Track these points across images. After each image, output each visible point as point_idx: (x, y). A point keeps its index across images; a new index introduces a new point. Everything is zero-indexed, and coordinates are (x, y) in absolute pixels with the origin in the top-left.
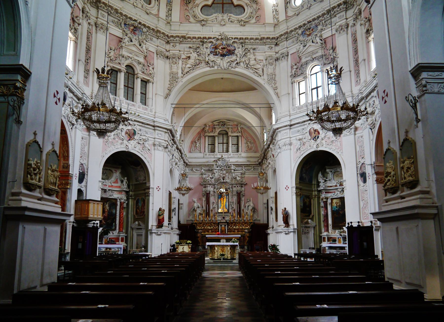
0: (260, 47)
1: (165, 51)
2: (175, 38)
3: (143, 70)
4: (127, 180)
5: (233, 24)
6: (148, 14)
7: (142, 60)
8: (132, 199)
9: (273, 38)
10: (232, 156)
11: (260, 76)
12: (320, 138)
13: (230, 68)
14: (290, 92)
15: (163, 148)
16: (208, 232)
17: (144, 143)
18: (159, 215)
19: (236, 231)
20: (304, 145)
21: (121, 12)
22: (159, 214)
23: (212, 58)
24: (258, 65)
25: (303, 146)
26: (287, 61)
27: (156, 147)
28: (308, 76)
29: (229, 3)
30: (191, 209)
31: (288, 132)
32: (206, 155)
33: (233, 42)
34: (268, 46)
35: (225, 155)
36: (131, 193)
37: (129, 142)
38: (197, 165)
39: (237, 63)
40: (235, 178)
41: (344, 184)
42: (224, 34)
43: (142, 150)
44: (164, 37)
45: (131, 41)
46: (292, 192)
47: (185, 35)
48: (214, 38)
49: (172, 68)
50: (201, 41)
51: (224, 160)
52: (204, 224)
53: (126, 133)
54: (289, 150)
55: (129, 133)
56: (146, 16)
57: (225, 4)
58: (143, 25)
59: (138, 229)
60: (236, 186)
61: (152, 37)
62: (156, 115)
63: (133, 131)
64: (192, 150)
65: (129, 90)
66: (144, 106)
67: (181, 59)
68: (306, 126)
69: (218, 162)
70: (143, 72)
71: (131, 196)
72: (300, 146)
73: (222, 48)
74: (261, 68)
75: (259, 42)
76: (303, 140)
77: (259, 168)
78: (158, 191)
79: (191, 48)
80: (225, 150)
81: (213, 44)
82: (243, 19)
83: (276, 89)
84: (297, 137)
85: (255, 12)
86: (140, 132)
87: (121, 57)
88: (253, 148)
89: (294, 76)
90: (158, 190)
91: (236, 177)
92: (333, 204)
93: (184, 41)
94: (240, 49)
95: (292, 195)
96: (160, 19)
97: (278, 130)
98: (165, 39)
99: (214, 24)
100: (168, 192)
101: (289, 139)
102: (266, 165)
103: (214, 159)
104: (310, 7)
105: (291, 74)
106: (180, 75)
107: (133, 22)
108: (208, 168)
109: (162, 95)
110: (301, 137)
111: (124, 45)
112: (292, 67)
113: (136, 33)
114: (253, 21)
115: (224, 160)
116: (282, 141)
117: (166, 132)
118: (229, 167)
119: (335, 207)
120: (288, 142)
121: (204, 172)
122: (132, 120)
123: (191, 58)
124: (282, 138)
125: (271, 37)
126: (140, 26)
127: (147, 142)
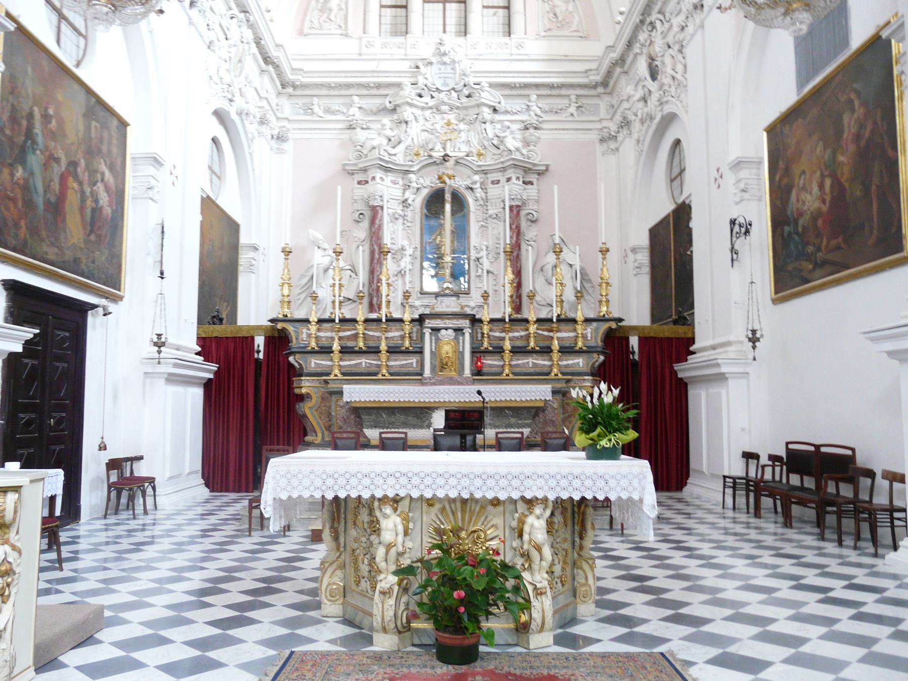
32: (369, 45)
38: (329, 86)
51: (446, 59)
60: (503, 180)
64: (307, 24)
69: (423, 69)
77: (603, 104)
80: (451, 27)
88: (576, 20)
91: (501, 140)
115: (446, 59)
118: (469, 96)
121: (358, 115)
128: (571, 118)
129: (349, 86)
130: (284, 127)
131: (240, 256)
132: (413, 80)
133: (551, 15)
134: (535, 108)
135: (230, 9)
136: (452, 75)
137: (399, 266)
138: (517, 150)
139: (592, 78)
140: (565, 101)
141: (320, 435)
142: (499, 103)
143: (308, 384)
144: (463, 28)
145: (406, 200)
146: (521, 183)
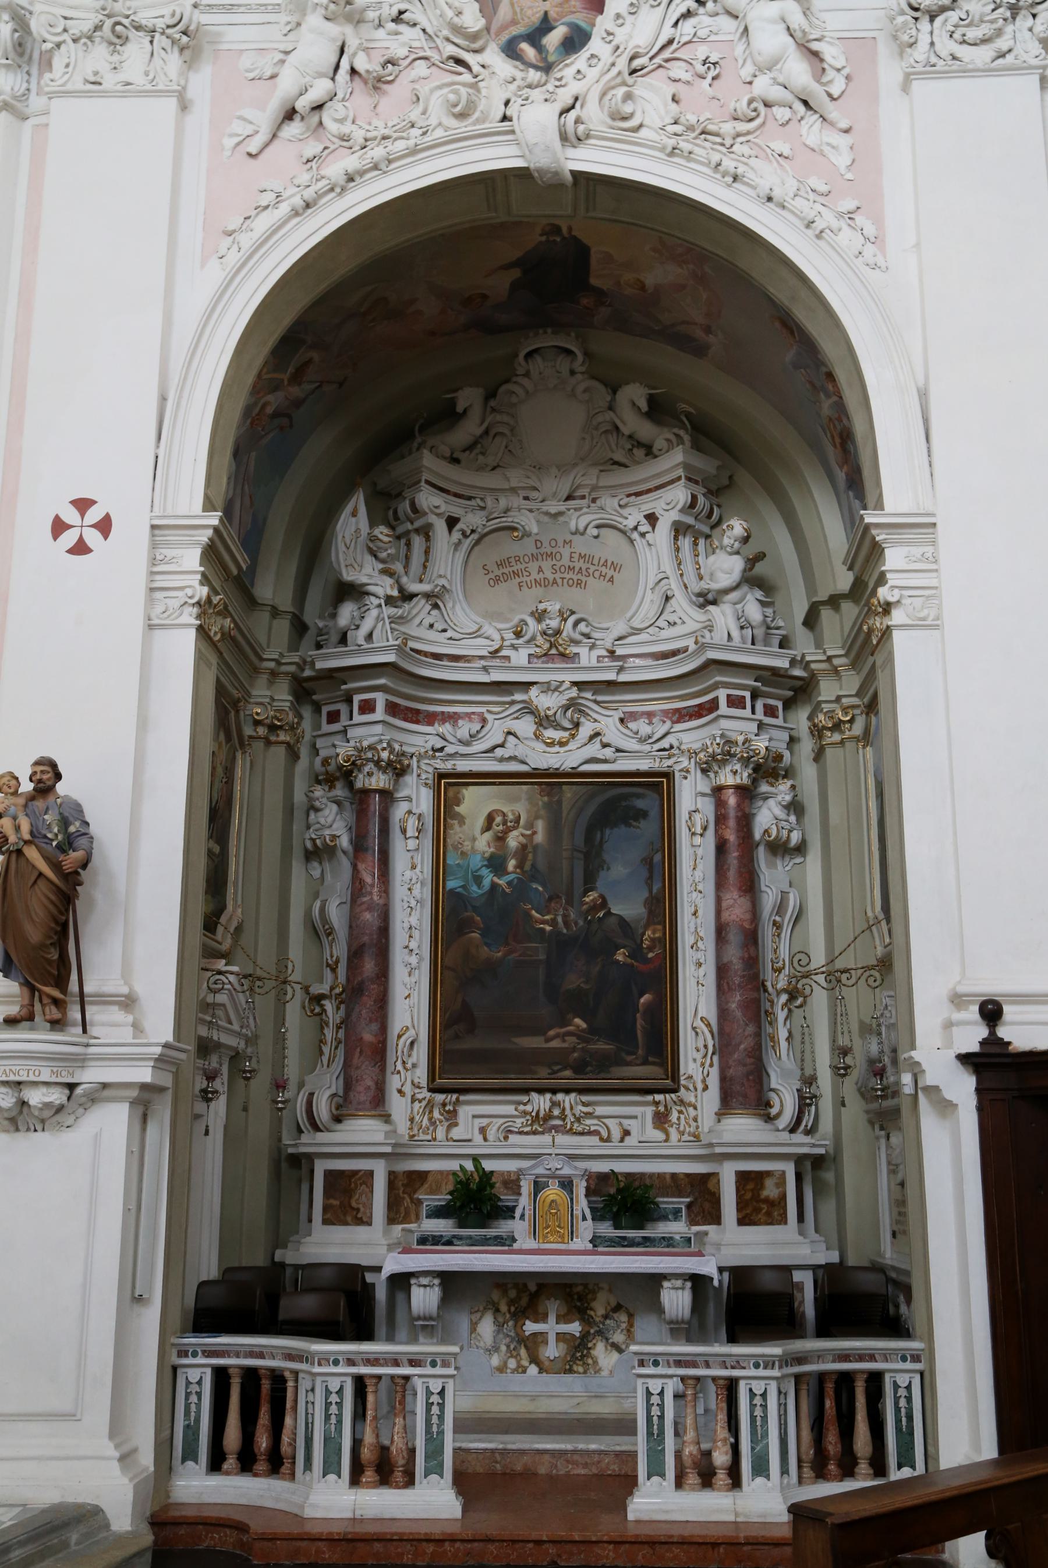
12: (595, 45)
41: (894, 558)
72: (320, 89)
92: (457, 833)
119: (476, 862)
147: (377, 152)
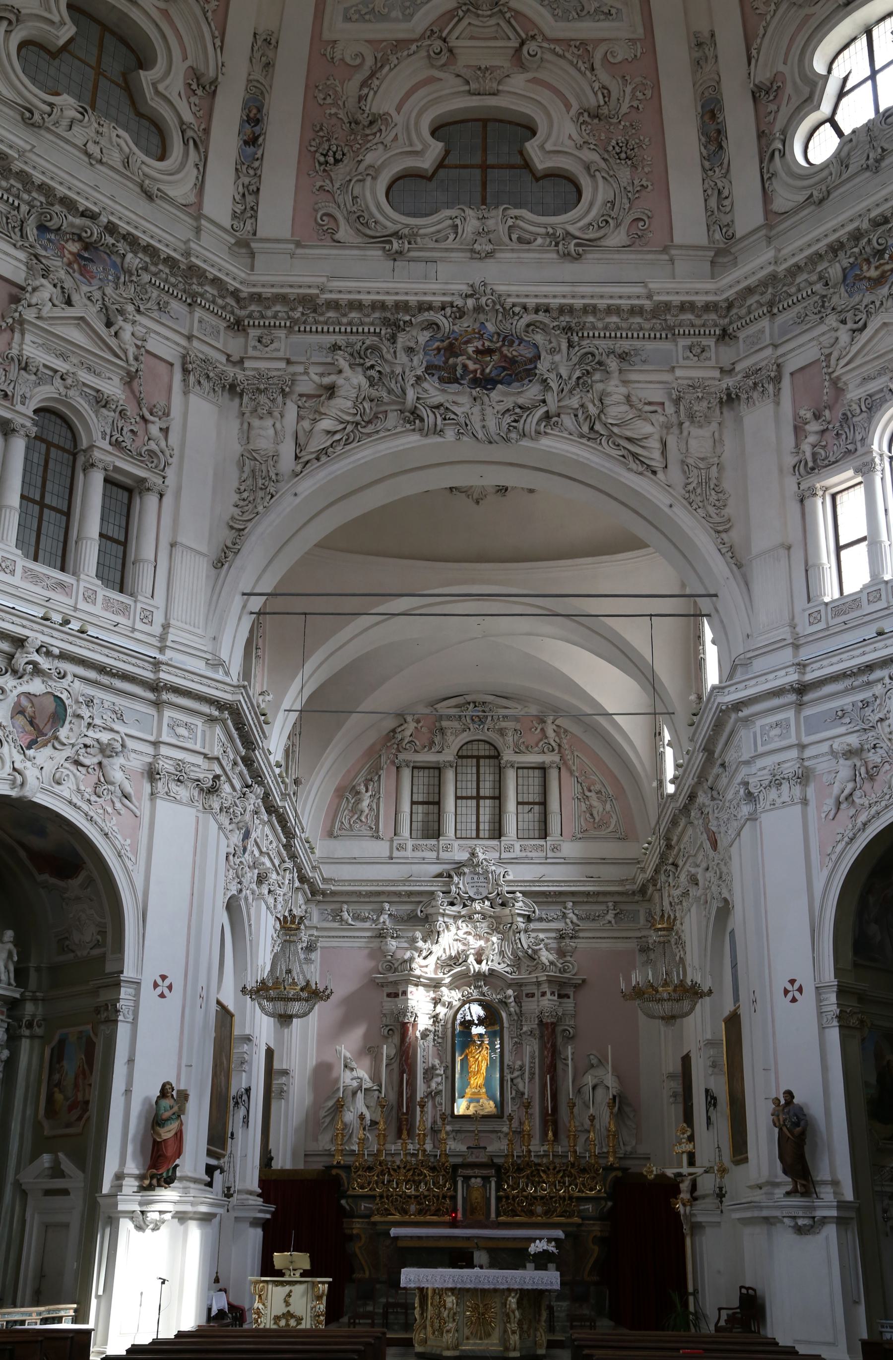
0: (650, 346)
1: (223, 359)
2: (269, 308)
3: (117, 435)
4: (17, 942)
5: (528, 251)
6: (149, 197)
7: (113, 388)
8: (32, 1037)
9: (708, 307)
10: (517, 853)
11: (649, 474)
13: (513, 435)
14: (794, 535)
15: (196, 793)
16: (405, 1212)
17: (105, 761)
18: (156, 1121)
19: (539, 1209)
20: (871, 778)
21: (22, 171)
22: (156, 1115)
23: (433, 392)
24: (639, 423)
25: (867, 786)
26: (777, 403)
27: (160, 784)
28: (877, 460)
29: (512, 167)
30: (329, 1098)
31: (787, 720)
32: (401, 848)
33: (528, 325)
34: (683, 342)
35: (486, 851)
36: (29, 1008)
37: (30, 753)
38: (359, 894)
39: (547, 416)
40: (532, 957)
42: (488, 291)
43: (94, 798)
44: (220, 301)
45: (69, 302)
46: (820, 1014)
47: (315, 291)
48: (443, 308)
49: (253, 433)
50: (386, 322)
52: (382, 1173)
53: (18, 711)
54: (799, 806)
55: (29, 710)
56: (143, 206)
57: (493, 167)
58: (124, 237)
59: (49, 1193)
61: (166, 298)
62: (171, 637)
63: (50, 706)
65: (45, 517)
66: (115, 595)
67: (295, 397)
68: (878, 689)
69: (456, 879)
70: (117, 444)
71: (30, 1025)
72: (850, 786)
73: (477, 351)
74: (657, 437)
75: (647, 326)
76: (865, 755)
78: (162, 996)
79: (340, 348)
80: (485, 826)
81: (439, 336)
82: (572, 229)
83: (726, 531)
84: (838, 740)
85: (625, 201)
86: (85, 712)
87: (14, 369)
89: (810, 464)
90: (159, 990)
91: (535, 952)
93: (311, 319)
94: (557, 358)
95: (822, 1028)
96: (203, 222)
97: (740, 714)
98: (223, 308)
99: (447, 250)
100: (214, 1007)
101: (794, 753)
102: (677, 892)
103: (437, 869)
104: (878, 161)
105: (796, 459)
106: (287, 462)
107: (78, 221)
108: (409, 907)
109: (204, 549)
110: (853, 740)
111: (29, 315)
112: (799, 430)
113: (88, 272)
114: (618, 237)
116: (760, 763)
117: (211, 720)
120: (790, 768)
121: (388, 924)
122: (48, 654)
123: (341, 392)
124: (761, 749)
125: (700, 299)
126: (110, 240)
127: (119, 761)
128: (608, 927)
129: (379, 893)
130: (312, 935)
131: (274, 1082)
132: (444, 889)
133: (588, 815)
134: (571, 915)
135: (284, 862)
136: (485, 884)
137: (429, 1087)
138: (552, 963)
139: (628, 887)
140: (603, 907)
141: (367, 1273)
142: (534, 912)
143: (358, 1226)
144: (497, 825)
145: (438, 1015)
146: (556, 998)
147: (873, 810)
